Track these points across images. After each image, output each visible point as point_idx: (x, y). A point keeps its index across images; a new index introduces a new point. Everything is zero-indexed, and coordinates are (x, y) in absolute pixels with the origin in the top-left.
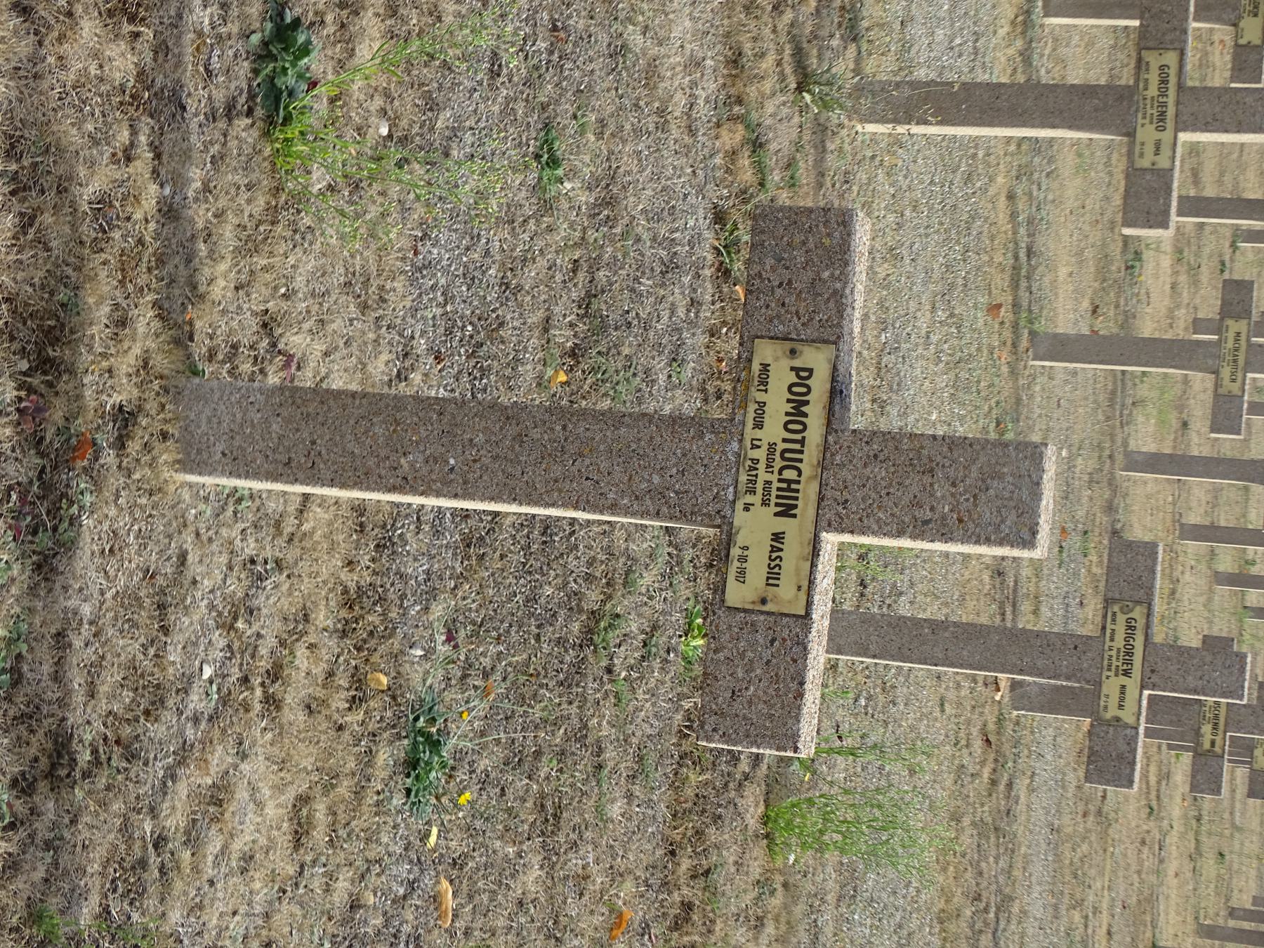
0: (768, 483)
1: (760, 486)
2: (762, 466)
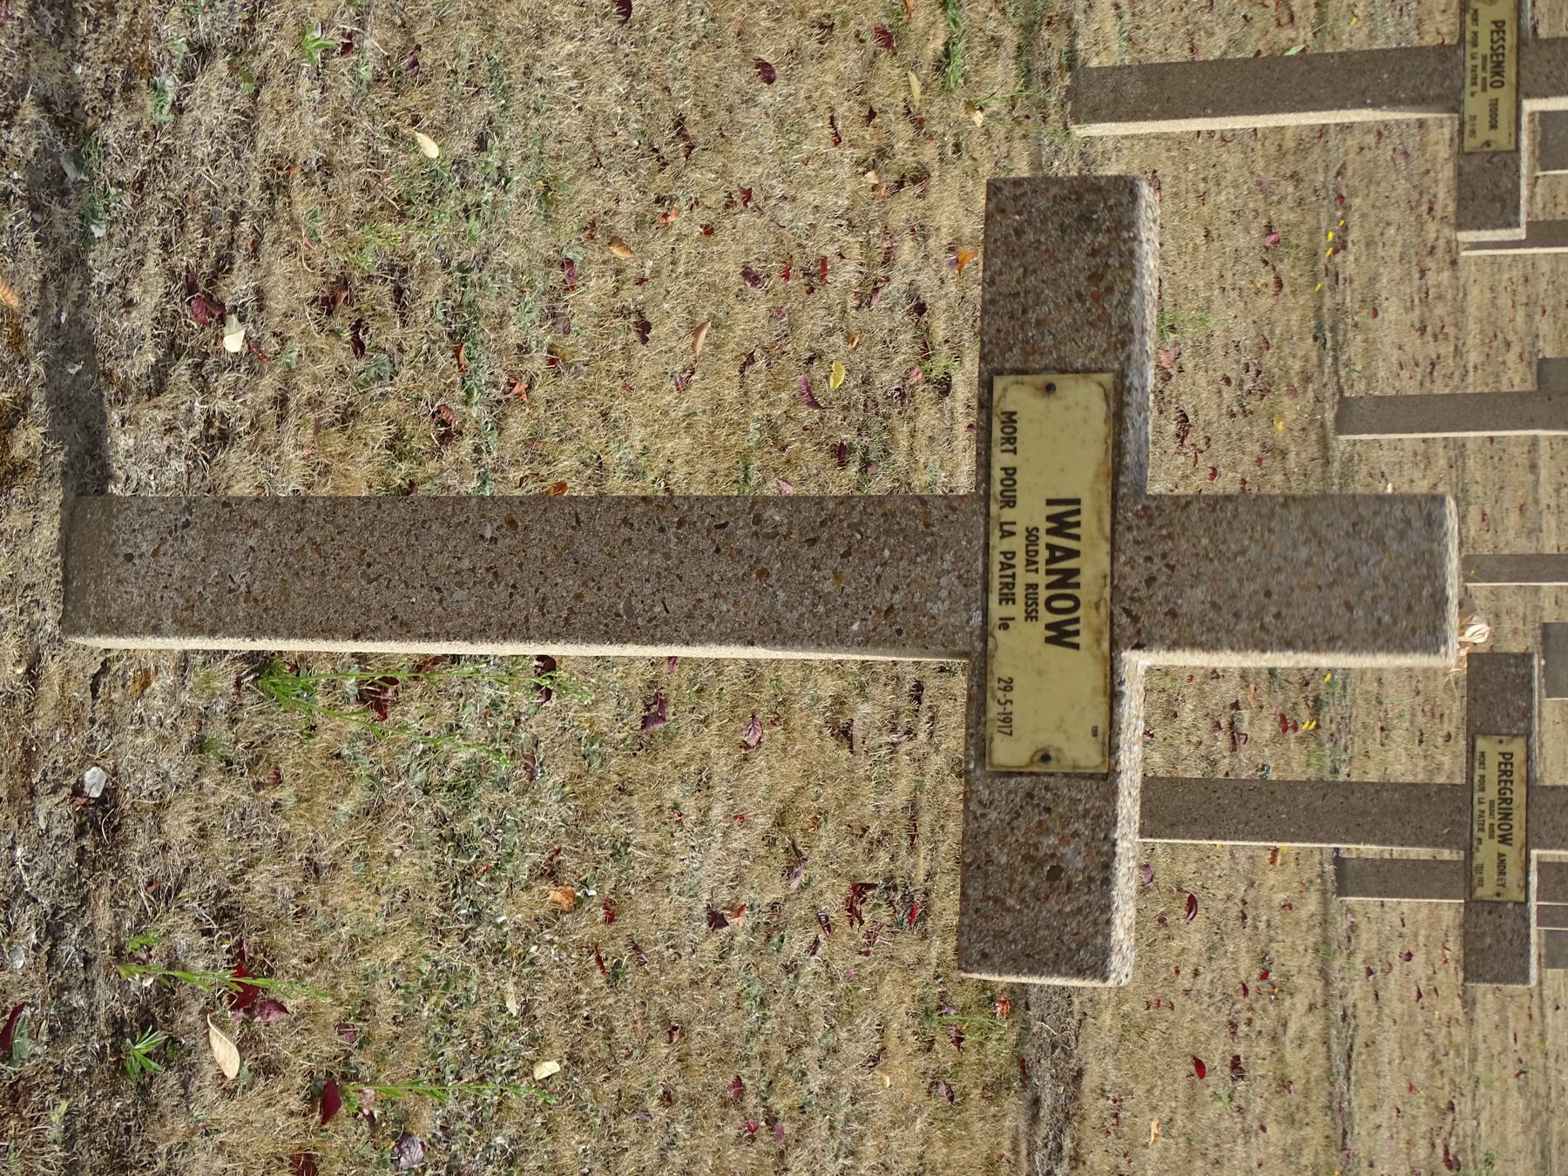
0: (1034, 586)
1: (1020, 591)
2: (1020, 560)
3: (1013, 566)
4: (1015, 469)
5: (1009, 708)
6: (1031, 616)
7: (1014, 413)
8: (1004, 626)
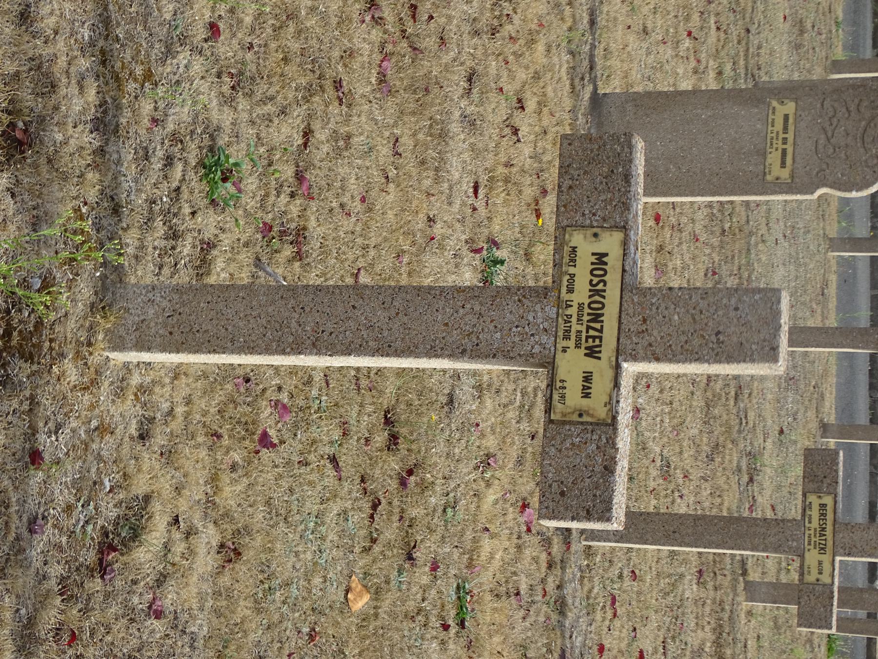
0: (580, 332)
2: (574, 319)
4: (574, 275)
6: (578, 346)
7: (576, 247)
8: (564, 350)
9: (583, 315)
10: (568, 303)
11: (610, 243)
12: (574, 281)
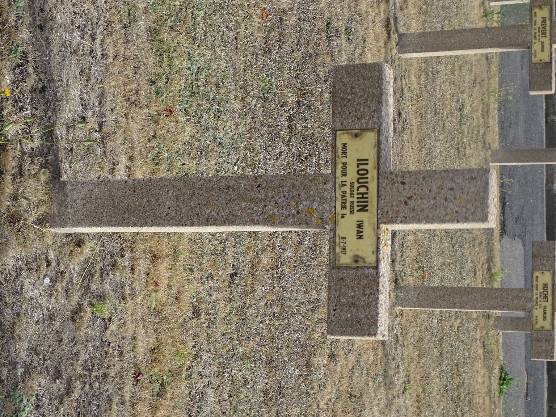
0: (353, 202)
1: (348, 205)
2: (348, 195)
3: (346, 196)
5: (345, 245)
6: (352, 212)
7: (346, 144)
8: (343, 216)
9: (354, 190)
10: (343, 183)
11: (371, 137)
12: (346, 167)
